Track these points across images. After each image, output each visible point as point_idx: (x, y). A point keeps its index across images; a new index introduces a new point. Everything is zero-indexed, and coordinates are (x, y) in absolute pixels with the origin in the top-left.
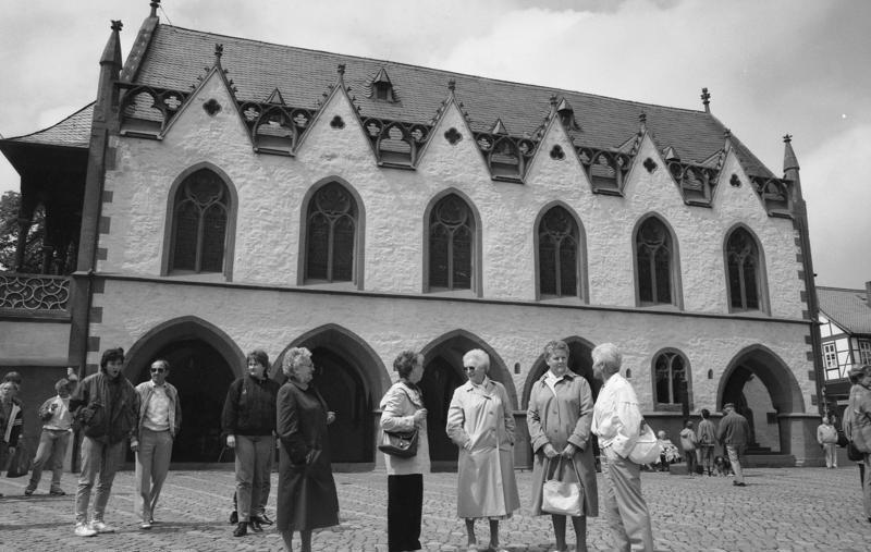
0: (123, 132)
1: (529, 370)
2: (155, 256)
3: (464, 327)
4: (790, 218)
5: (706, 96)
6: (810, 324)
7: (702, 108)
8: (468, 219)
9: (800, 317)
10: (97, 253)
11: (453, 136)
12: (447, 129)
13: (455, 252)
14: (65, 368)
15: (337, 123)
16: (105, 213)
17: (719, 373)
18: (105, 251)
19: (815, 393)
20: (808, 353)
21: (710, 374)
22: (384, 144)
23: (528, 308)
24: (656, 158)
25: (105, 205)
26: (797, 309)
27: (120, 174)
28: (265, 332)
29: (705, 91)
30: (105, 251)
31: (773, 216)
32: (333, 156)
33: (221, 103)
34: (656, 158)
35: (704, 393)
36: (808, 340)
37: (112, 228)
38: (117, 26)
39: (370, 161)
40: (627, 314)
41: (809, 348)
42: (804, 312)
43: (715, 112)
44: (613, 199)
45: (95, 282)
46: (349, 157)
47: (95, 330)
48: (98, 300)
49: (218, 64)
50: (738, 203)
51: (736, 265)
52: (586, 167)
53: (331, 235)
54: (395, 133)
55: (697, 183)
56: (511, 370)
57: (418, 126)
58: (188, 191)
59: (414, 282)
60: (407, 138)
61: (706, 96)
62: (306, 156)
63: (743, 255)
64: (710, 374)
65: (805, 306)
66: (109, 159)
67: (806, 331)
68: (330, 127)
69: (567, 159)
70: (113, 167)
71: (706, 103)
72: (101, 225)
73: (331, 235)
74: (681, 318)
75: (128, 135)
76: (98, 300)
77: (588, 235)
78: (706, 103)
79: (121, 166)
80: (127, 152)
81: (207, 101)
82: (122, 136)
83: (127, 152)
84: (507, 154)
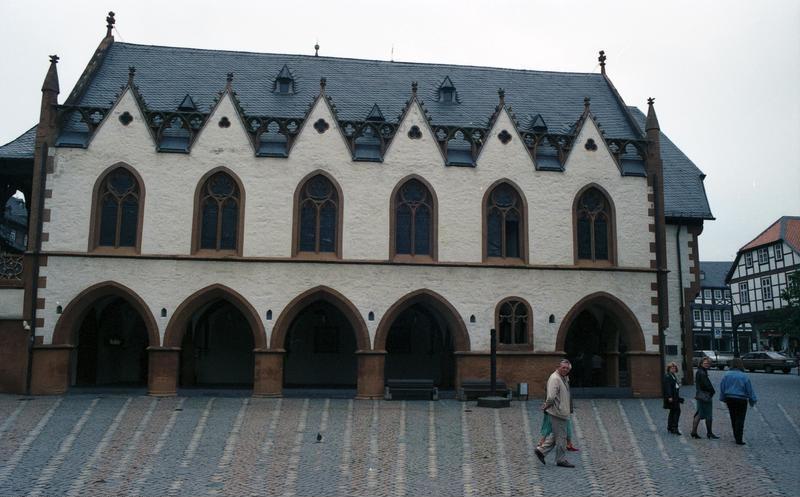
0: (58, 144)
1: (380, 318)
2: (83, 237)
3: (326, 283)
4: (644, 176)
5: (602, 58)
6: (657, 272)
7: (598, 70)
8: (333, 195)
9: (647, 265)
11: (321, 126)
12: (316, 120)
13: (322, 223)
14: (22, 321)
15: (225, 123)
16: (46, 206)
17: (560, 318)
18: (48, 234)
19: (657, 333)
20: (653, 298)
21: (552, 319)
22: (265, 136)
23: (384, 267)
24: (511, 131)
25: (47, 200)
26: (646, 259)
27: (56, 176)
28: (164, 292)
29: (602, 53)
30: (48, 234)
31: (625, 174)
32: (221, 150)
33: (132, 114)
34: (511, 131)
35: (545, 336)
36: (654, 287)
39: (250, 152)
40: (475, 269)
41: (655, 294)
43: (609, 74)
44: (467, 169)
45: (41, 258)
46: (233, 151)
47: (41, 293)
48: (43, 272)
49: (130, 83)
50: (591, 164)
51: (589, 220)
52: (441, 144)
53: (220, 214)
54: (274, 127)
55: (549, 146)
56: (365, 317)
57: (293, 120)
58: (109, 186)
59: (284, 246)
60: (283, 130)
61: (602, 58)
62: (196, 150)
63: (595, 213)
64: (552, 319)
65: (653, 256)
66: (48, 166)
67: (653, 278)
68: (218, 128)
69: (424, 137)
70: (52, 171)
71: (603, 65)
73: (220, 214)
74: (525, 271)
75: (61, 146)
76: (43, 272)
77: (440, 202)
78: (603, 65)
79: (57, 172)
80: (62, 158)
81: (122, 113)
82: (57, 147)
83: (62, 158)
84: (369, 136)
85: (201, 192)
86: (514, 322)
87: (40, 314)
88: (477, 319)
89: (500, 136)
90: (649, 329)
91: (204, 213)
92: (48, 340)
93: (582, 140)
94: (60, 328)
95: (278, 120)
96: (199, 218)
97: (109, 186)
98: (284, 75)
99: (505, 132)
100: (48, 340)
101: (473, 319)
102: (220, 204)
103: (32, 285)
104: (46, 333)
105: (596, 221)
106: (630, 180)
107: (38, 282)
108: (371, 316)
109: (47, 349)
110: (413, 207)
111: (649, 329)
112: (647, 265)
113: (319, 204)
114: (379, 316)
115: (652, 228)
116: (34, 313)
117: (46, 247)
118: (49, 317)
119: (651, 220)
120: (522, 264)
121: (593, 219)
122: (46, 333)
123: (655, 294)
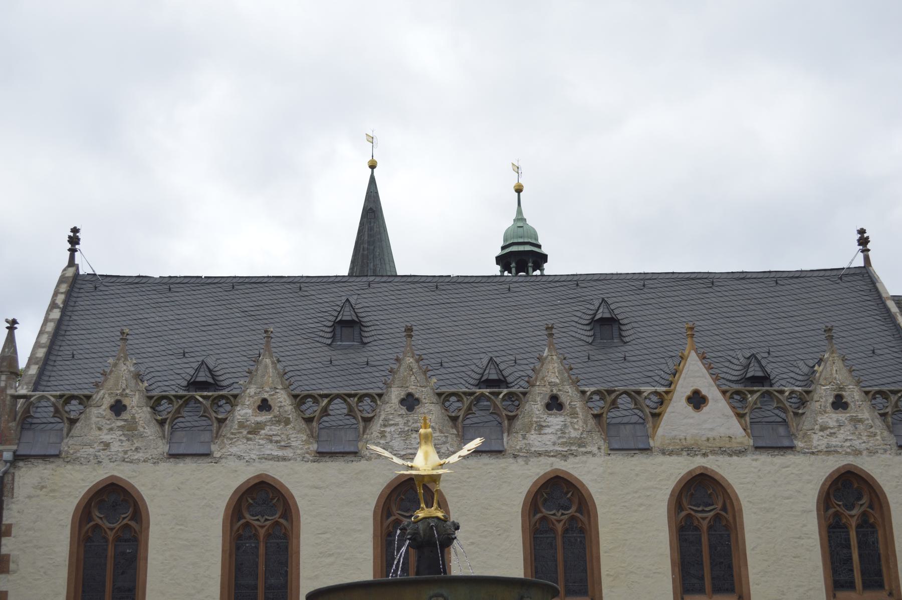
5: (863, 241)
7: (859, 262)
24: (711, 391)
29: (862, 232)
38: (12, 325)
43: (877, 267)
61: (863, 241)
71: (865, 251)
78: (865, 251)
89: (690, 400)
91: (238, 548)
93: (824, 394)
95: (344, 397)
96: (230, 556)
98: (347, 316)
99: (696, 393)
102: (262, 532)
121: (853, 523)
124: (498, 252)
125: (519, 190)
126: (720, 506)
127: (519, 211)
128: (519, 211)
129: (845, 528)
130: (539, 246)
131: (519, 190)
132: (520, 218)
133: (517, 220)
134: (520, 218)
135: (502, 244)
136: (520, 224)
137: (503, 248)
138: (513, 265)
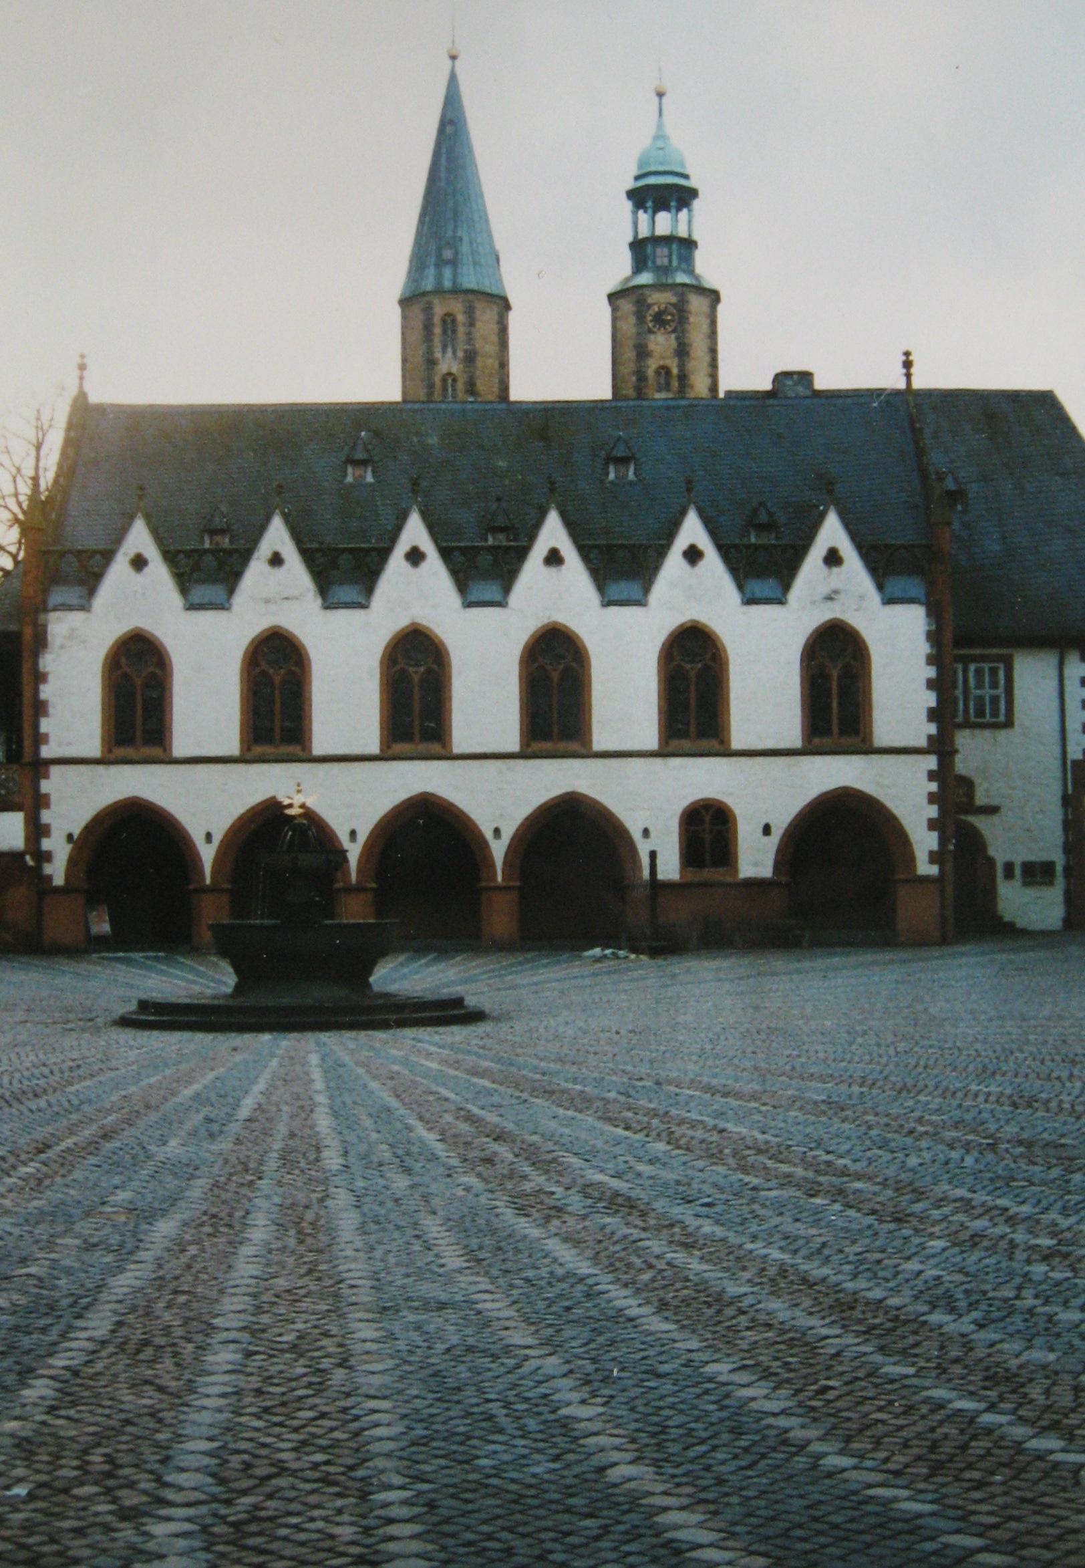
4: (920, 603)
10: (39, 739)
15: (276, 560)
21: (767, 830)
26: (921, 731)
35: (755, 858)
36: (932, 776)
37: (51, 710)
41: (934, 787)
42: (930, 737)
45: (41, 767)
47: (46, 816)
48: (45, 786)
58: (123, 661)
64: (767, 830)
66: (41, 641)
67: (931, 762)
72: (40, 708)
76: (45, 786)
85: (250, 664)
86: (707, 837)
87: (46, 844)
88: (651, 829)
90: (924, 842)
92: (59, 880)
94: (72, 862)
97: (123, 661)
100: (59, 880)
101: (646, 833)
103: (33, 806)
104: (57, 871)
105: (840, 677)
106: (899, 609)
107: (40, 801)
108: (497, 832)
109: (58, 890)
110: (555, 670)
111: (924, 842)
112: (923, 743)
113: (416, 673)
114: (508, 833)
115: (931, 684)
116: (37, 842)
117: (46, 752)
118: (58, 848)
119: (931, 672)
120: (722, 749)
122: (57, 871)
123: (934, 787)
124: (630, 184)
125: (660, 95)
126: (708, 656)
127: (660, 126)
128: (660, 126)
129: (827, 678)
130: (686, 177)
131: (660, 95)
132: (660, 136)
133: (656, 138)
134: (660, 136)
135: (634, 171)
136: (660, 144)
137: (637, 178)
138: (649, 204)
